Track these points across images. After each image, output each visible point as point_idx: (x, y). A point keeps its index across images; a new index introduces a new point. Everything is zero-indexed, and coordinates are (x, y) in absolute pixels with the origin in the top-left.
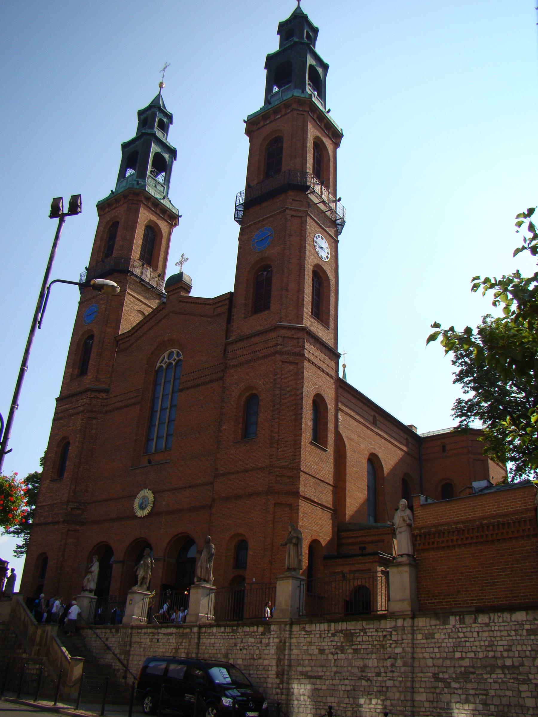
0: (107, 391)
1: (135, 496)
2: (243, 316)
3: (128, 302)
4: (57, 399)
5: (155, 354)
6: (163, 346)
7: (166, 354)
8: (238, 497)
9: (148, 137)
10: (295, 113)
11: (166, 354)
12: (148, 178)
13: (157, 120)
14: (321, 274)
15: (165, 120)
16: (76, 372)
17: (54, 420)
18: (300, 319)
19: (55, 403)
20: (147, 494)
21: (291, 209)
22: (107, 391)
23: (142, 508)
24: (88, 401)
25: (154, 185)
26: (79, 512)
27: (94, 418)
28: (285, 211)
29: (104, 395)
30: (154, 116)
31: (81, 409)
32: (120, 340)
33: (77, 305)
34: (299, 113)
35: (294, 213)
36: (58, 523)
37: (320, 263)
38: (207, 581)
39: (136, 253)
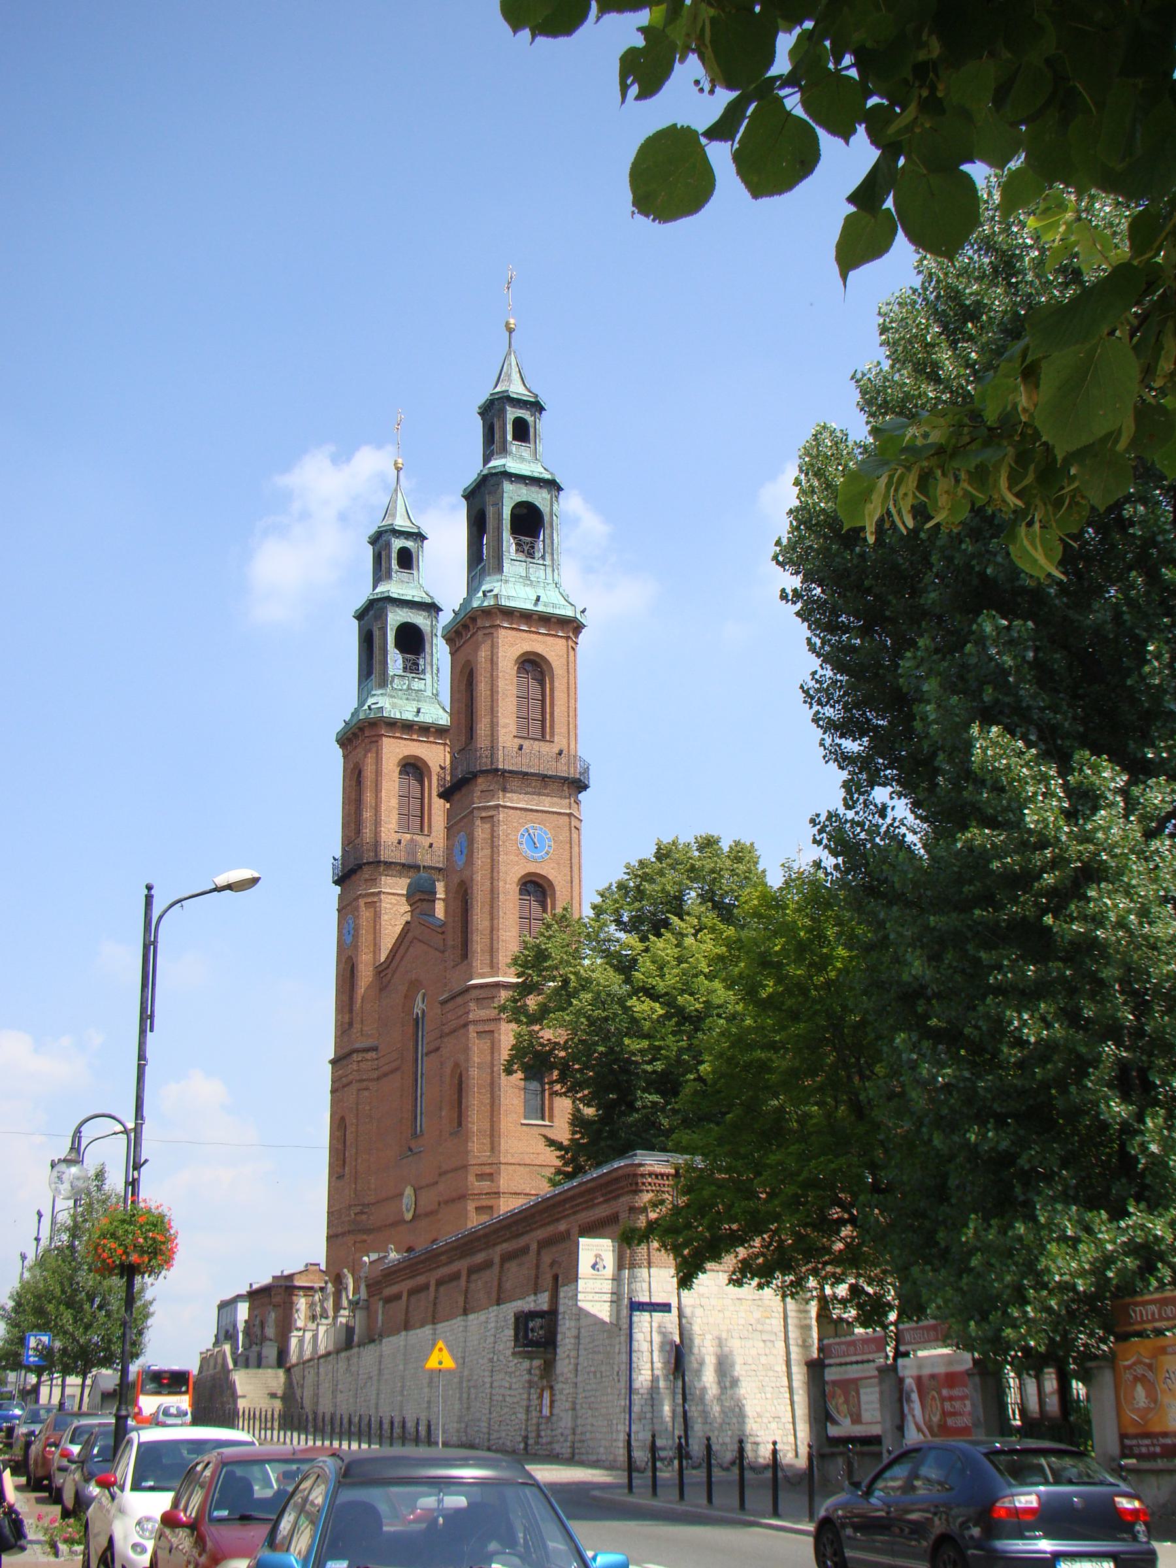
0: (375, 1049)
1: (402, 1195)
2: (452, 964)
3: (388, 906)
4: (333, 1062)
5: (409, 998)
6: (415, 985)
7: (420, 997)
8: (453, 1200)
9: (380, 604)
10: (480, 633)
11: (420, 997)
12: (392, 682)
13: (394, 555)
14: (541, 882)
15: (409, 544)
16: (347, 1016)
17: (333, 1091)
18: (494, 968)
19: (329, 1068)
20: (409, 1191)
21: (479, 808)
22: (375, 1049)
23: (408, 1211)
24: (355, 1067)
25: (405, 687)
26: (364, 1217)
27: (367, 1089)
28: (472, 812)
29: (373, 1054)
30: (388, 545)
31: (351, 1077)
32: (380, 972)
33: (335, 915)
34: (487, 631)
35: (484, 814)
36: (343, 1234)
37: (532, 868)
38: (327, 1318)
39: (390, 823)
